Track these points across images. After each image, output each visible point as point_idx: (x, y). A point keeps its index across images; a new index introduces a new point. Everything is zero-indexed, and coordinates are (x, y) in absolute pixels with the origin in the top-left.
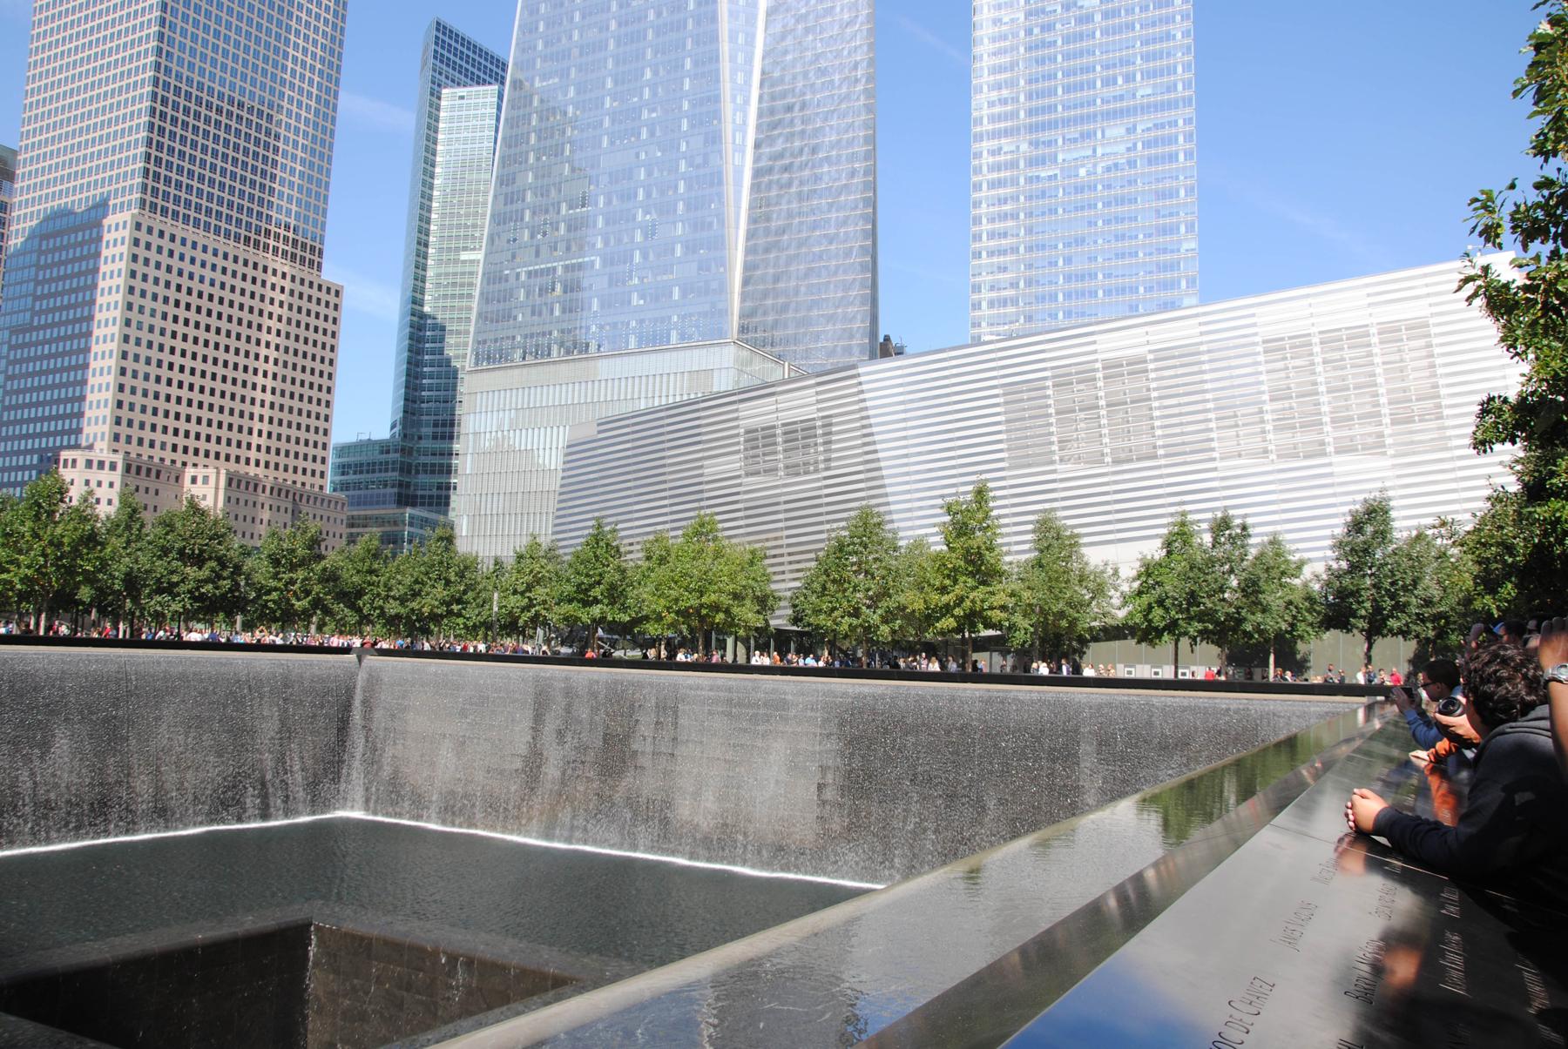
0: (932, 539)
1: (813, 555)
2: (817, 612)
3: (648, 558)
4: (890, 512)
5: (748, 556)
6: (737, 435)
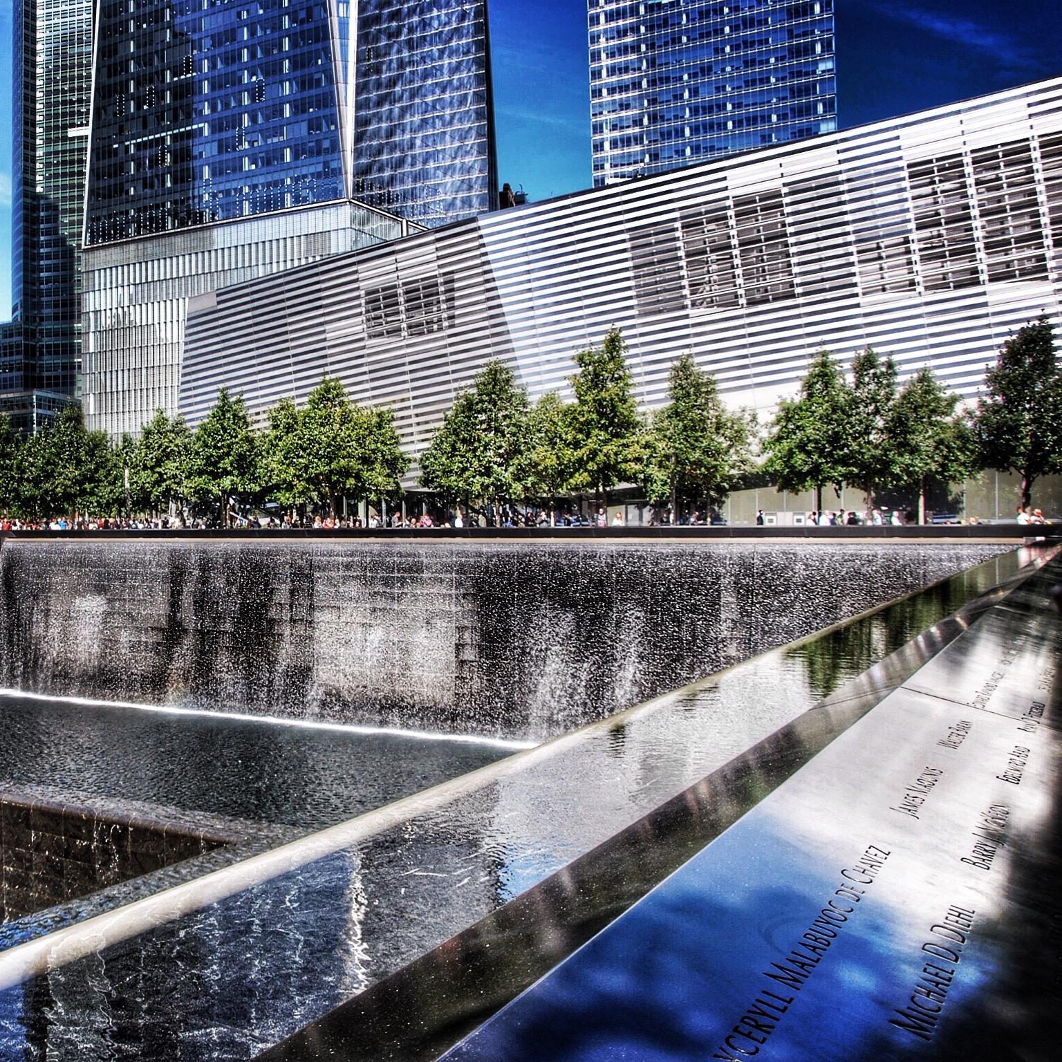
0: (563, 393)
1: (441, 415)
2: (447, 472)
3: (275, 427)
4: (518, 368)
5: (375, 420)
6: (358, 297)
